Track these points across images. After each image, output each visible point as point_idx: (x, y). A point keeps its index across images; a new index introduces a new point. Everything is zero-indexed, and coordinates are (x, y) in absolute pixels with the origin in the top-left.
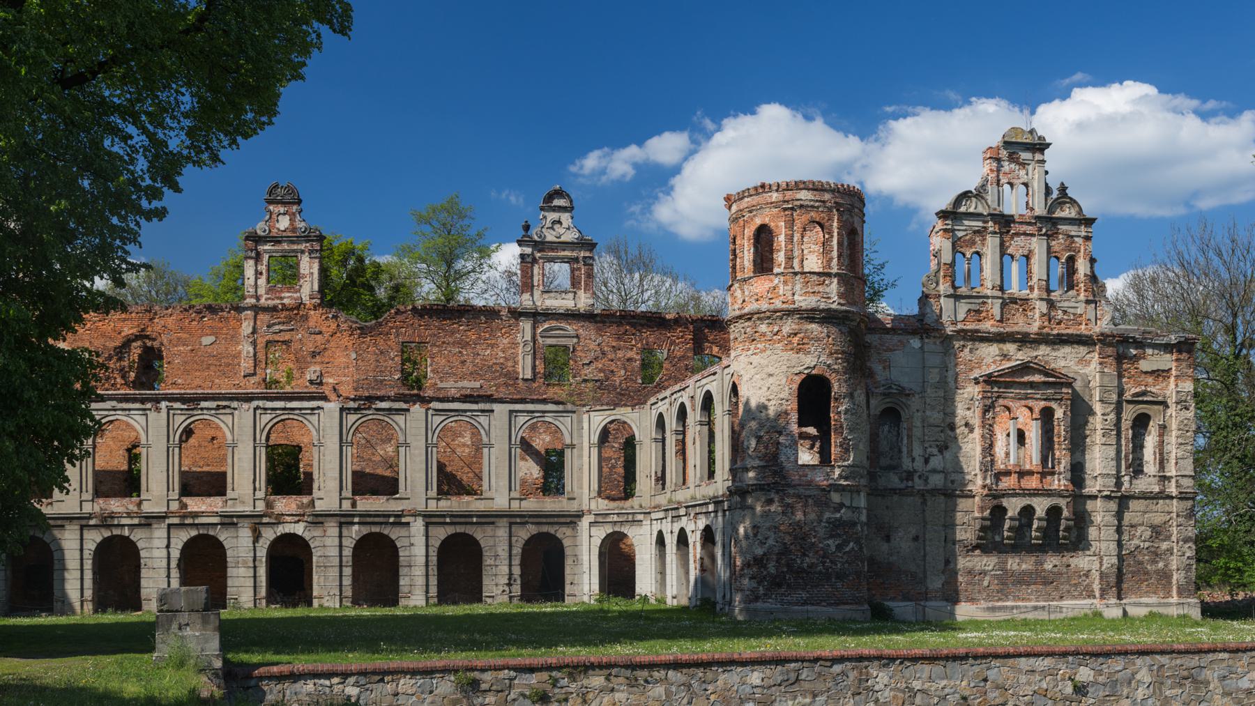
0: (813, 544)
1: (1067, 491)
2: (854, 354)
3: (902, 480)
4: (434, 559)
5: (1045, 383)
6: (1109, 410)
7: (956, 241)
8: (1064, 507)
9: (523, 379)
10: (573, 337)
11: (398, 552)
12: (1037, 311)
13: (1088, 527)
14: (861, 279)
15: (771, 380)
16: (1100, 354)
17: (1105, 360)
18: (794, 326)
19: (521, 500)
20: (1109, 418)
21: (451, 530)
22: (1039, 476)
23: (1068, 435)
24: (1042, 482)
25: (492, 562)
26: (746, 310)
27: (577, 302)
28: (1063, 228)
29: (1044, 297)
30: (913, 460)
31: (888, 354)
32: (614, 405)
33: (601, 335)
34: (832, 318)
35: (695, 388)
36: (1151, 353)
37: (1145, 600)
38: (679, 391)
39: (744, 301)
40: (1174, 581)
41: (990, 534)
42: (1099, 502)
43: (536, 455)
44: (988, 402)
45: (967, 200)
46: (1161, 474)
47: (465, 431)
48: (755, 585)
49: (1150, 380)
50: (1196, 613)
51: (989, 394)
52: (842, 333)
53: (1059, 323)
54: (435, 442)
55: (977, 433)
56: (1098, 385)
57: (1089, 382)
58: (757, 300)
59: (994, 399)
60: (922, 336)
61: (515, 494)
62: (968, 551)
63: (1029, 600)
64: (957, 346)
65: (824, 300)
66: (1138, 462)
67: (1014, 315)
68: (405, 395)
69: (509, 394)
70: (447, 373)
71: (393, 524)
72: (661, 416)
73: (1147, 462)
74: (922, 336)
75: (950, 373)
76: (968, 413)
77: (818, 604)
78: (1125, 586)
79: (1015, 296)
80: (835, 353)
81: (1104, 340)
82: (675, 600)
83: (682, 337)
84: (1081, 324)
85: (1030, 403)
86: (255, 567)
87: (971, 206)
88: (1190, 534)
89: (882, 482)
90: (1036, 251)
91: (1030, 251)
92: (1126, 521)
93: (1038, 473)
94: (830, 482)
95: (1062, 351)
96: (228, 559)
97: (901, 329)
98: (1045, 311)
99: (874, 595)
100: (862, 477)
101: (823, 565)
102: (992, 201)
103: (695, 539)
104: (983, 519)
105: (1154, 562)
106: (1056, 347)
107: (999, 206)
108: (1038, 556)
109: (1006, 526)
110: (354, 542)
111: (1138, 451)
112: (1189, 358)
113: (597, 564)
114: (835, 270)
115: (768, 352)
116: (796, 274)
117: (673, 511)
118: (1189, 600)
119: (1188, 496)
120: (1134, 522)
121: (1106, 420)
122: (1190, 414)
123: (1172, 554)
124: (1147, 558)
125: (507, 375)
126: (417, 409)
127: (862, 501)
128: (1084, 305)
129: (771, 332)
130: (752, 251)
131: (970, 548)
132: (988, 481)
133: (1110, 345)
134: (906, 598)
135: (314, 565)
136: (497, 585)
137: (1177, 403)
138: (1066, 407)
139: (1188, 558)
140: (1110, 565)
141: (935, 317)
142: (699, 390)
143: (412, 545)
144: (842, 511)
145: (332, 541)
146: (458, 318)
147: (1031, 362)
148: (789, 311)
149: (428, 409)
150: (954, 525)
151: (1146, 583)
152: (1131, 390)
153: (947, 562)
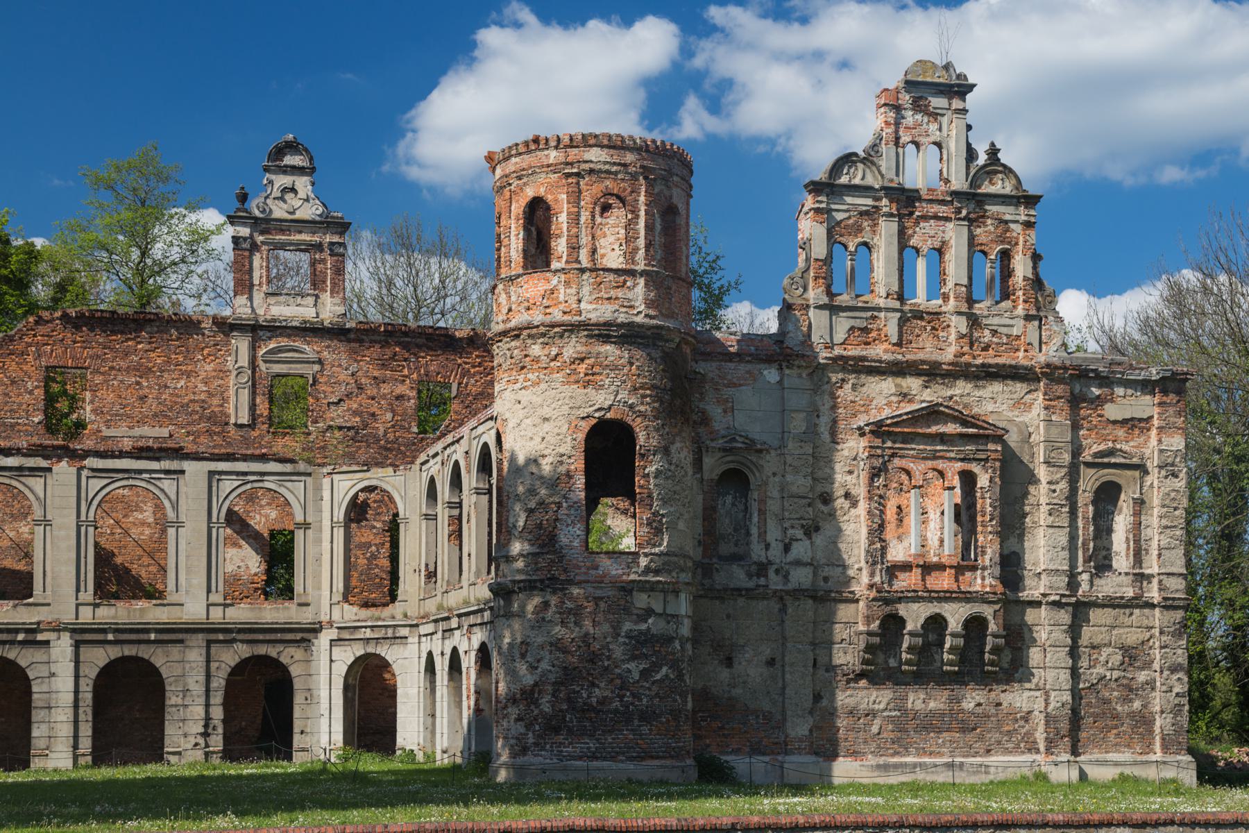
0: (606, 669)
1: (995, 593)
2: (671, 390)
3: (750, 576)
4: (87, 697)
5: (962, 436)
6: (1059, 476)
7: (833, 227)
8: (990, 618)
9: (235, 425)
10: (314, 362)
11: (30, 687)
12: (953, 330)
13: (1029, 648)
14: (683, 280)
15: (547, 427)
16: (1045, 394)
17: (1053, 403)
18: (580, 348)
19: (226, 606)
20: (1058, 487)
21: (115, 652)
22: (953, 571)
23: (997, 513)
24: (957, 580)
25: (179, 701)
26: (512, 324)
27: (320, 311)
28: (992, 209)
29: (963, 310)
30: (767, 546)
31: (731, 391)
32: (368, 465)
33: (356, 360)
34: (637, 337)
35: (470, 439)
36: (1122, 394)
37: (1112, 756)
38: (453, 444)
39: (510, 310)
40: (1157, 730)
41: (881, 657)
42: (1043, 611)
43: (255, 539)
44: (877, 463)
45: (850, 167)
46: (1137, 571)
47: (145, 503)
48: (523, 730)
49: (1121, 433)
50: (1189, 777)
51: (879, 452)
52: (651, 359)
53: (986, 349)
54: (91, 518)
55: (863, 506)
56: (1042, 439)
57: (1030, 435)
58: (528, 309)
59: (886, 458)
60: (781, 366)
61: (216, 598)
62: (848, 682)
63: (940, 754)
64: (834, 380)
65: (624, 310)
66: (1104, 553)
67: (918, 336)
68: (45, 447)
69: (214, 447)
70: (116, 415)
71: (24, 643)
72: (432, 481)
73: (1117, 554)
74: (781, 366)
75: (824, 421)
76: (849, 478)
77: (613, 759)
78: (1083, 735)
79: (921, 308)
80: (641, 388)
81: (1052, 373)
82: (446, 756)
83: (480, 365)
84: (1018, 350)
85: (940, 465)
87: (856, 176)
88: (1180, 660)
89: (720, 579)
90: (953, 242)
91: (943, 243)
92: (1084, 640)
93: (951, 567)
94: (633, 577)
95: (990, 388)
97: (750, 355)
98: (964, 330)
99: (708, 746)
100: (682, 570)
101: (621, 701)
102: (888, 169)
103: (469, 662)
104: (869, 634)
105: (1126, 700)
106: (981, 383)
107: (897, 175)
108: (953, 690)
109: (905, 645)
111: (1105, 537)
112: (1178, 401)
113: (341, 702)
114: (641, 266)
115: (543, 386)
116: (582, 271)
117: (444, 622)
118: (1179, 758)
119: (1176, 603)
120: (1097, 640)
121: (1054, 491)
122: (1180, 483)
123: (1153, 689)
124: (1115, 693)
125: (212, 418)
126: (64, 470)
127: (683, 606)
128: (1022, 322)
129: (547, 356)
130: (521, 236)
131: (851, 676)
132: (877, 579)
133: (1060, 381)
134: (756, 750)
136: (185, 735)
137: (1160, 467)
138: (994, 471)
139: (1177, 695)
140: (1059, 704)
141: (801, 338)
142: (475, 442)
144: (650, 621)
146: (135, 331)
147: (941, 405)
148: (572, 325)
149: (80, 469)
150: (830, 643)
151: (1115, 731)
152: (1092, 447)
153: (817, 697)
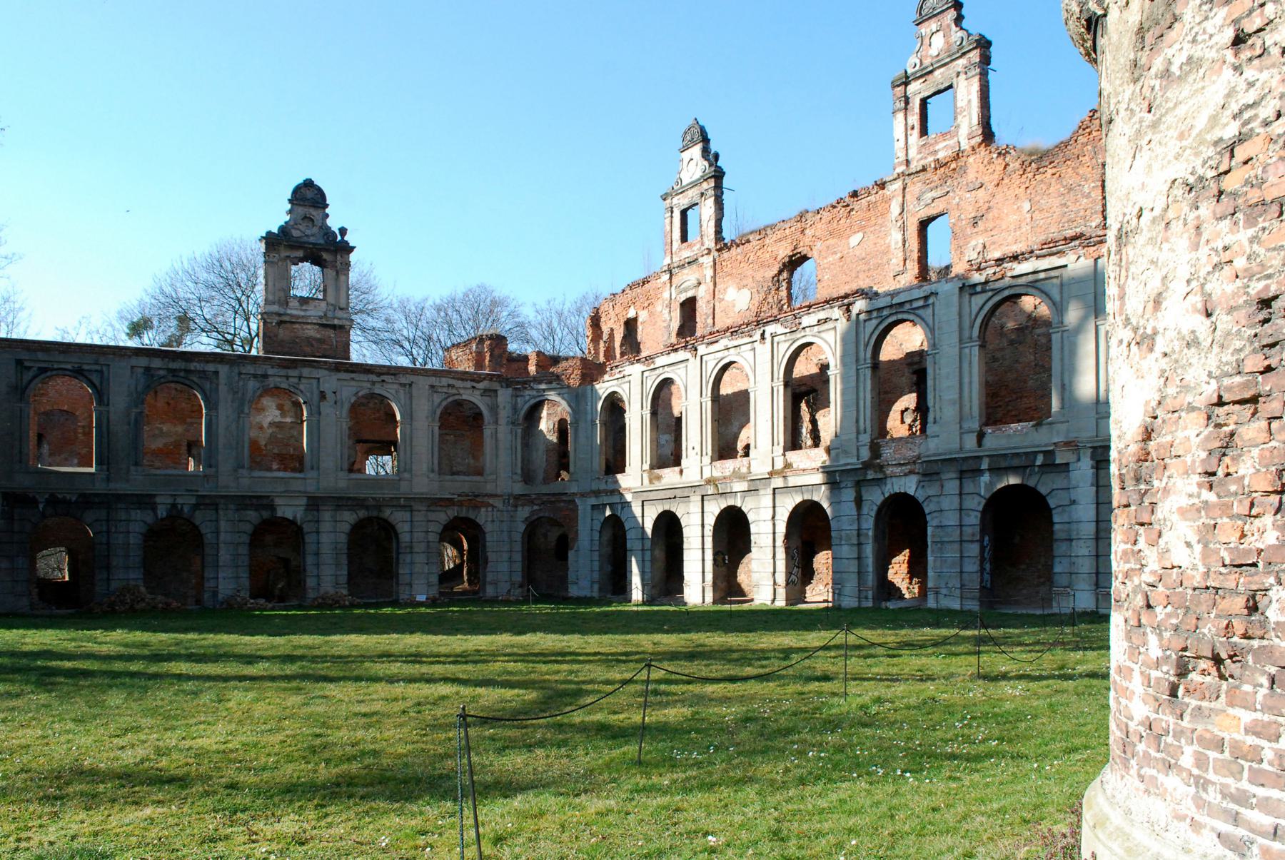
11: (1050, 517)
86: (859, 544)
96: (833, 534)
110: (984, 502)
135: (929, 540)
143: (1074, 502)
145: (950, 503)
